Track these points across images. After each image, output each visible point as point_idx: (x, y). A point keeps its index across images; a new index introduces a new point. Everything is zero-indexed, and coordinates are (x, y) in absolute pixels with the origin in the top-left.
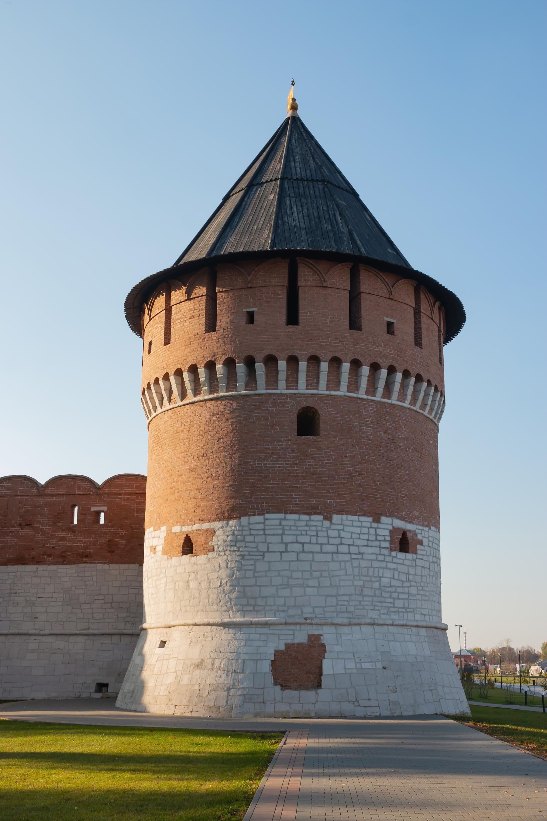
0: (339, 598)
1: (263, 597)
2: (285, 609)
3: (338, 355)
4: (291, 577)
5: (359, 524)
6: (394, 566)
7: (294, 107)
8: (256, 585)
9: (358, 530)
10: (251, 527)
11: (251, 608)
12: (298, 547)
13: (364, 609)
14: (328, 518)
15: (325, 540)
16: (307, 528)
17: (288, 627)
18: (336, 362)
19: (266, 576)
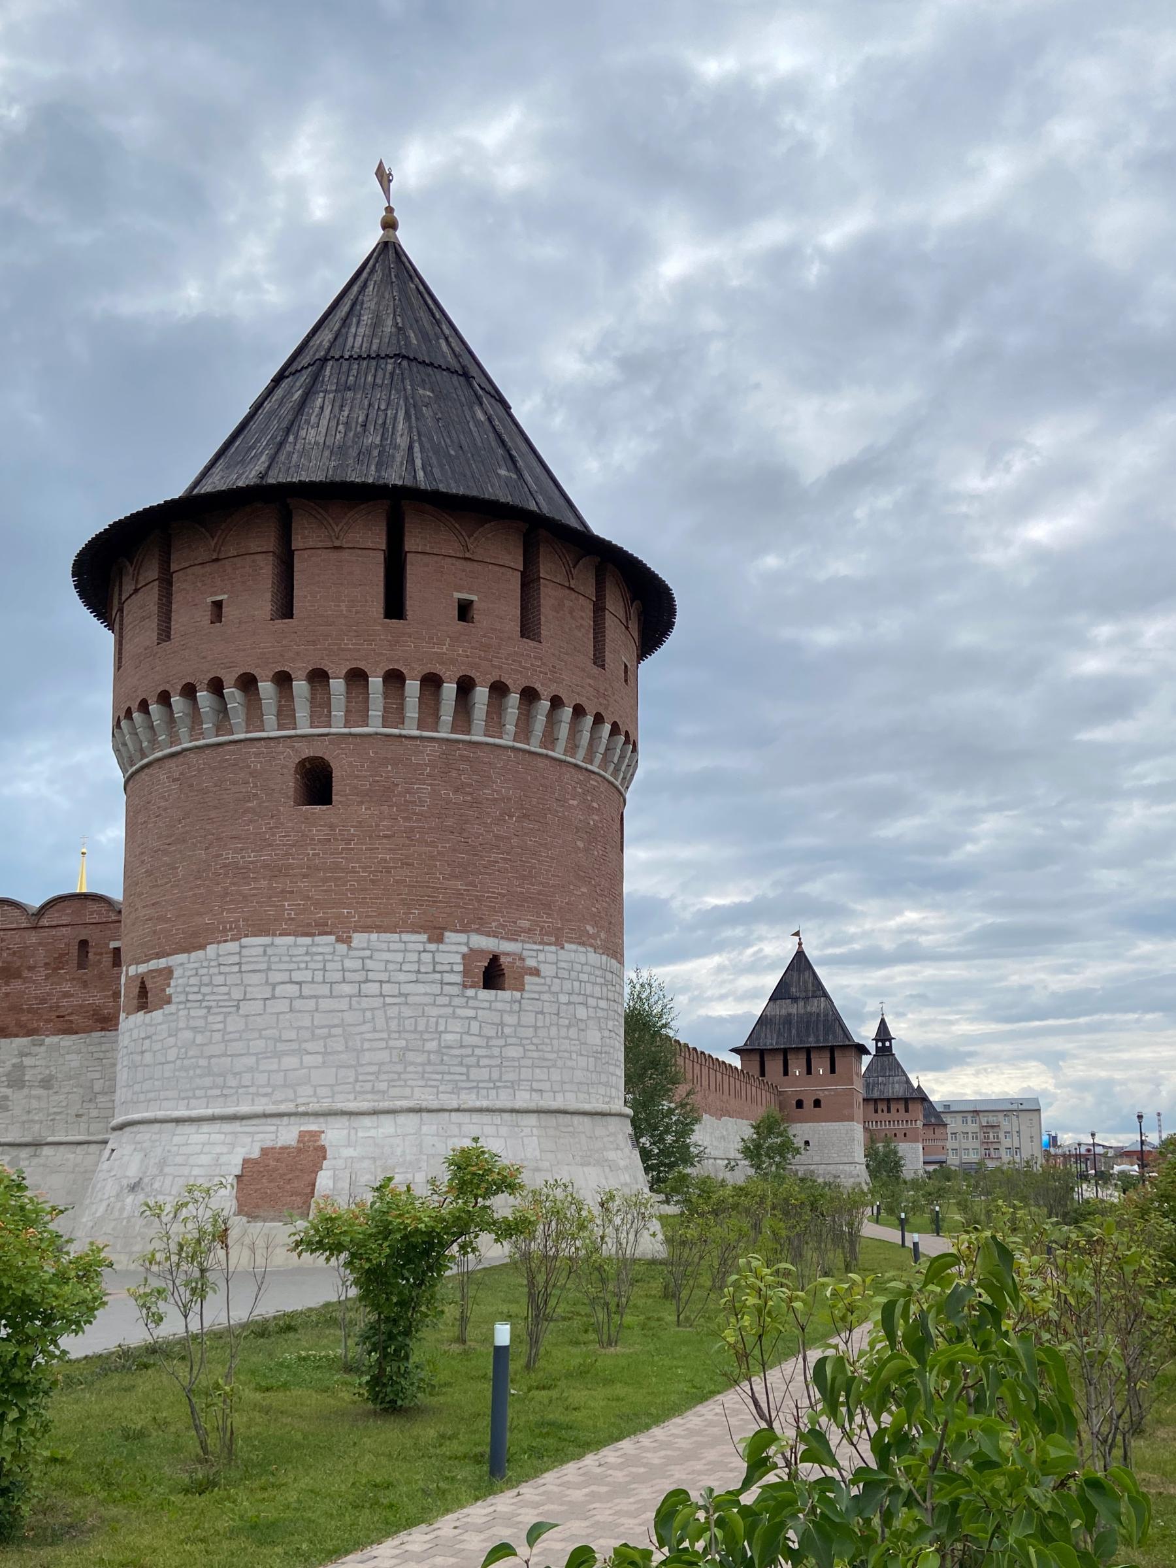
0: (360, 1070)
1: (236, 1074)
2: (269, 1090)
3: (362, 665)
4: (280, 1040)
5: (401, 946)
6: (471, 1013)
7: (389, 224)
8: (225, 1055)
9: (399, 957)
11: (218, 1092)
12: (292, 990)
14: (347, 941)
15: (338, 976)
16: (308, 958)
17: (269, 1120)
18: (357, 677)
19: (240, 1039)
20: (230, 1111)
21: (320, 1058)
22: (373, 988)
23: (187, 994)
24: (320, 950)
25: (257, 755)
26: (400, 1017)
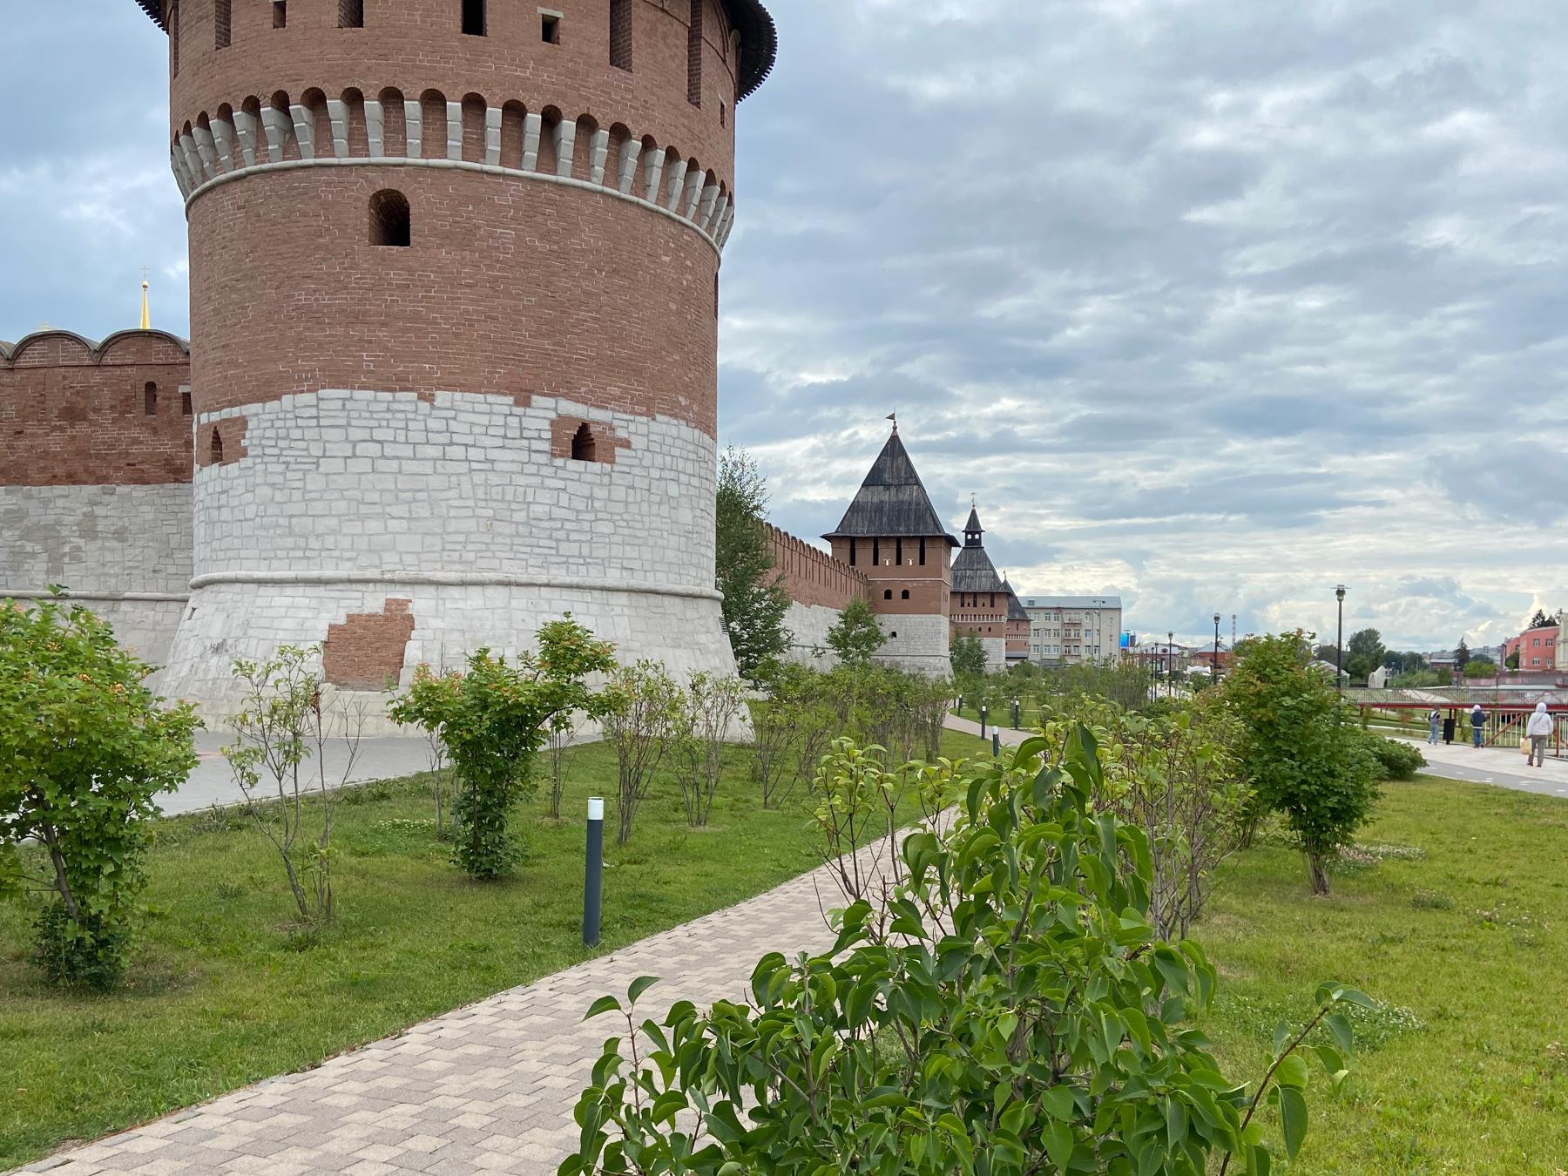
1: (318, 536)
2: (354, 555)
3: (438, 86)
5: (486, 408)
9: (484, 420)
10: (298, 412)
11: (301, 554)
12: (374, 449)
13: (494, 557)
14: (430, 399)
15: (421, 437)
16: (389, 416)
17: (354, 586)
18: (433, 100)
20: (314, 573)
21: (405, 524)
22: (458, 452)
23: (264, 447)
24: (402, 407)
25: (328, 184)
26: (486, 484)
